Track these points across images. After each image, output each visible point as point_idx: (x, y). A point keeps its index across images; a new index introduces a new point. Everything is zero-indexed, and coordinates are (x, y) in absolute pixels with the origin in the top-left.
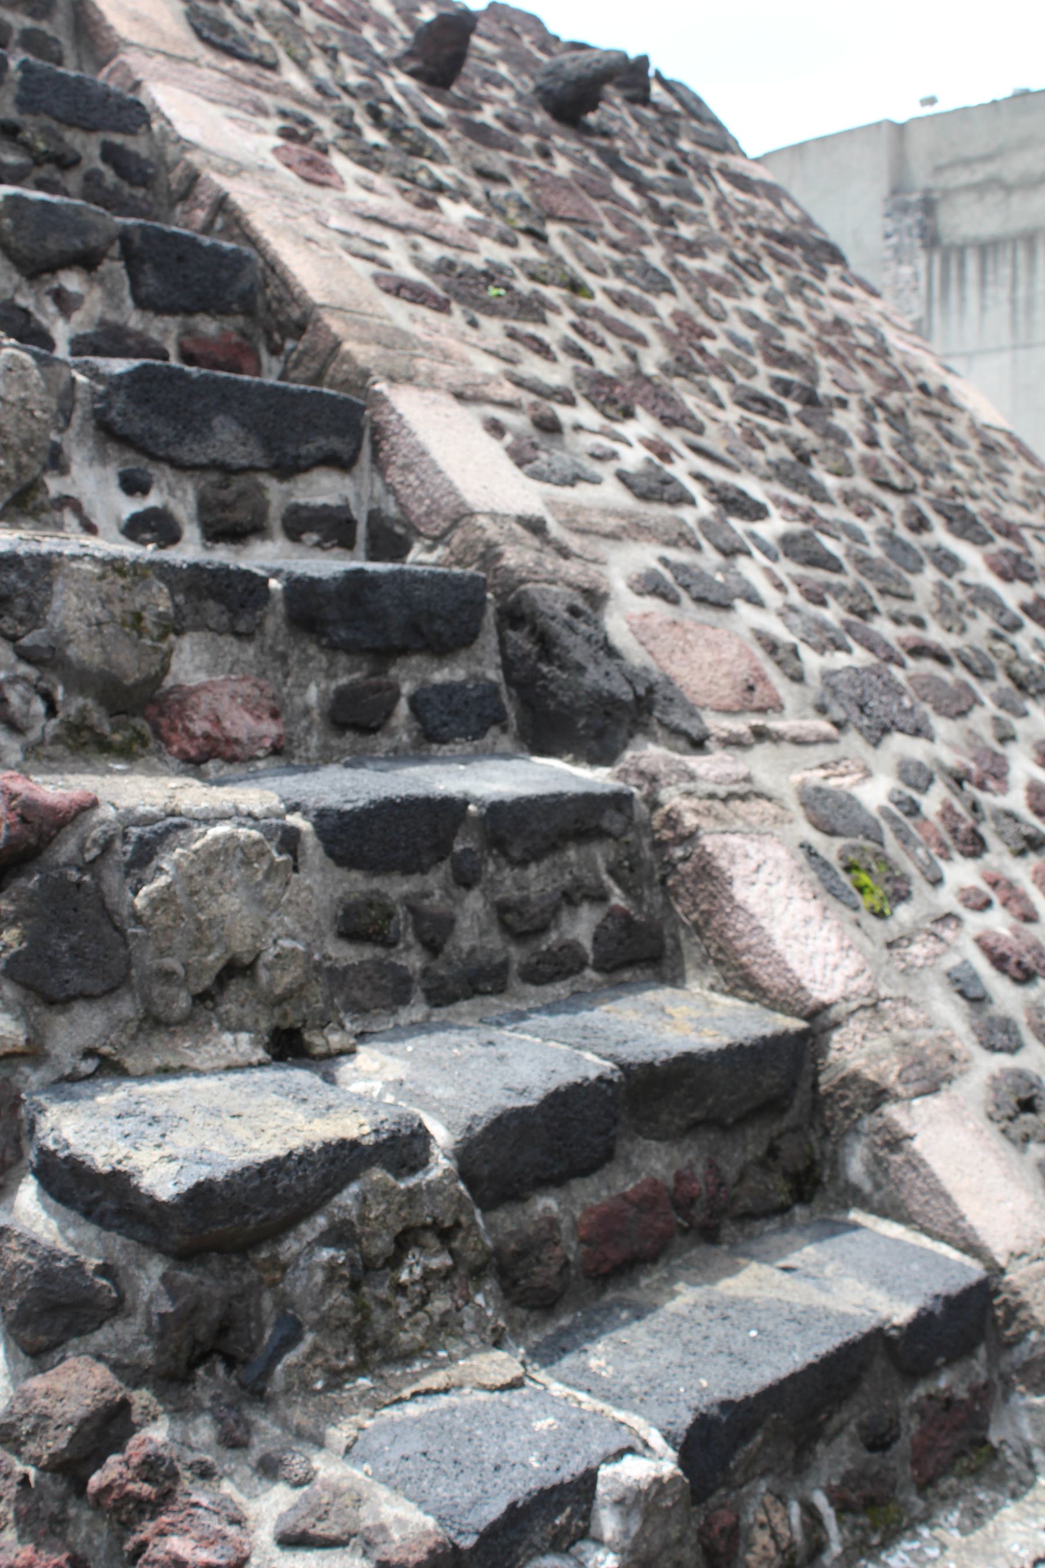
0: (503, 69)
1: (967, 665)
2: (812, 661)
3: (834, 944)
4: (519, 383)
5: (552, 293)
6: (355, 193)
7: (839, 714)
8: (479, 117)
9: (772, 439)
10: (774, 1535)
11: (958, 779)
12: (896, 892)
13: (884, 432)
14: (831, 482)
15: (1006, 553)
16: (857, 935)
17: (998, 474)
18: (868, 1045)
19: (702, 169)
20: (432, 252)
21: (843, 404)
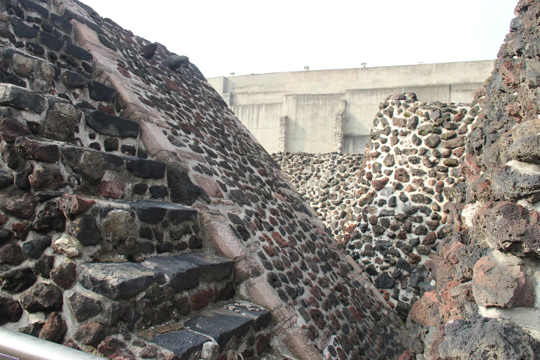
0: (159, 57)
1: (256, 192)
2: (229, 188)
3: (237, 245)
4: (169, 124)
5: (173, 106)
6: (134, 80)
8: (155, 66)
13: (237, 143)
14: (229, 152)
15: (262, 170)
17: (259, 153)
19: (199, 83)
20: (150, 94)
21: (229, 136)
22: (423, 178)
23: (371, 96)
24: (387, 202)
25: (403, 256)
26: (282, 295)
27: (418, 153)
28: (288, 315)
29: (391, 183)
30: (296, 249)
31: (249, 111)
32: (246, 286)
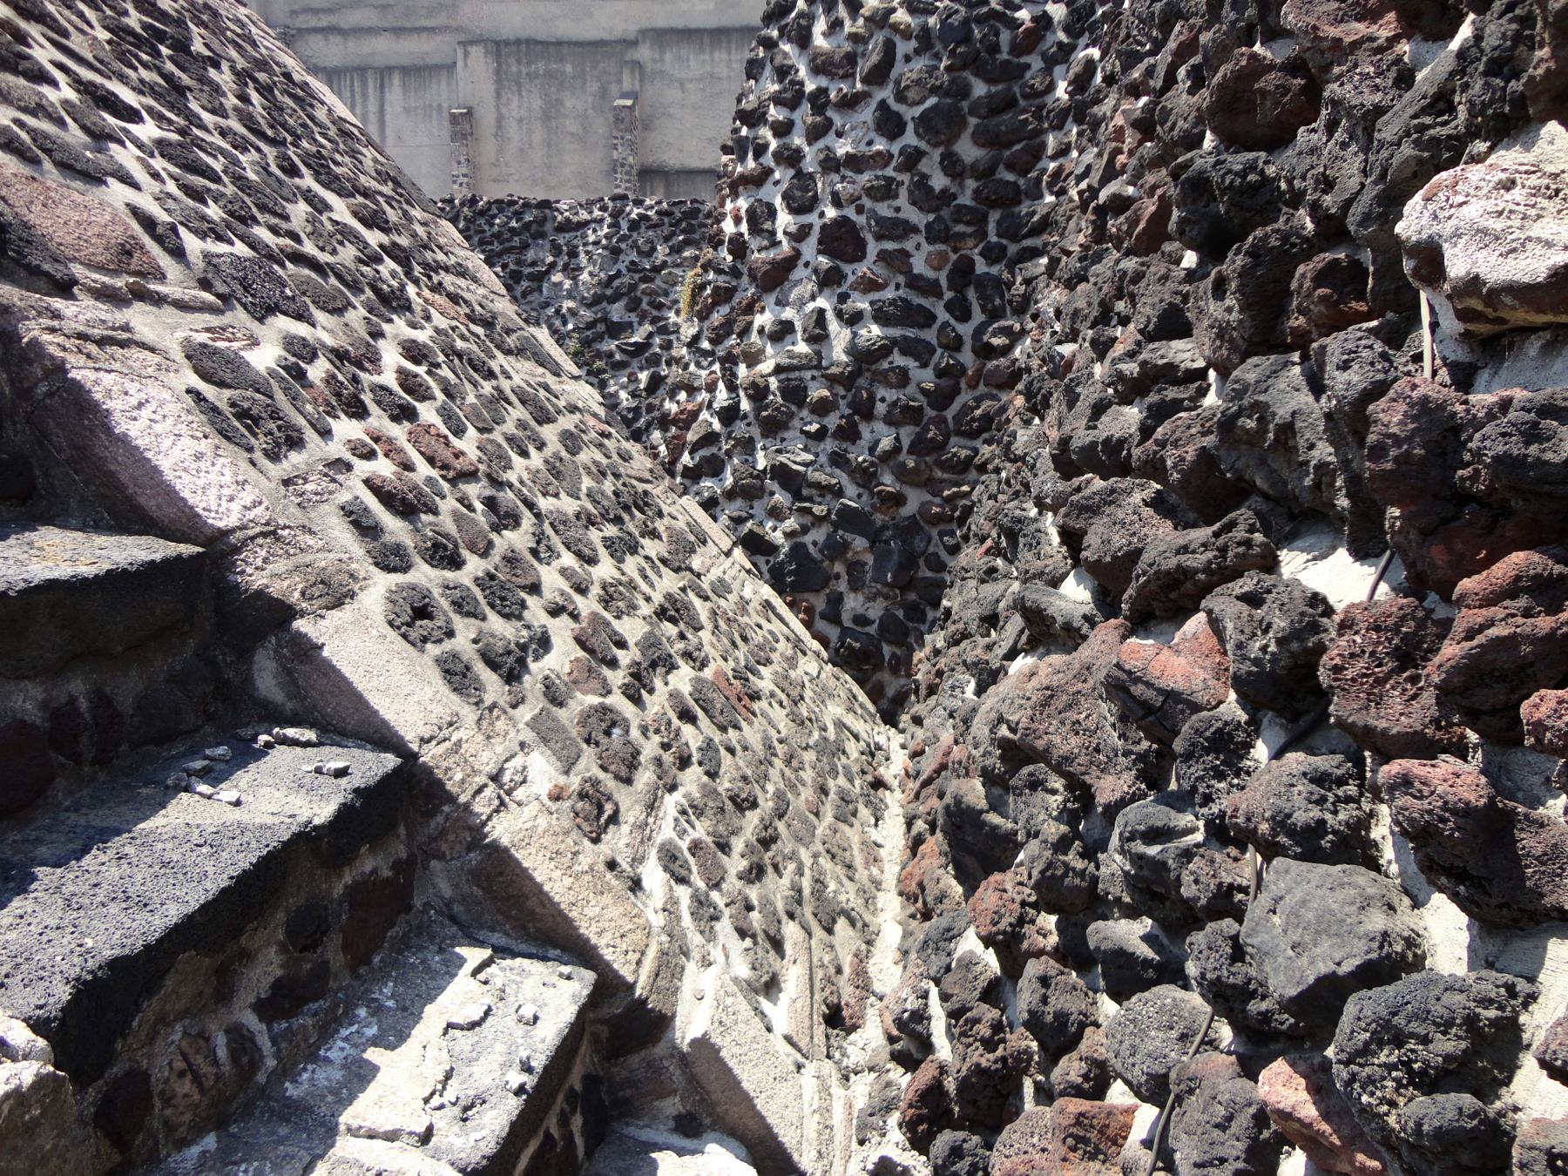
2: (193, 244)
3: (228, 479)
7: (222, 288)
9: (145, 65)
10: (197, 1079)
11: (339, 356)
12: (289, 438)
13: (255, 97)
14: (207, 117)
15: (366, 206)
16: (253, 474)
18: (270, 567)
21: (217, 66)
22: (909, 245)
23: (711, 53)
24: (798, 326)
25: (851, 489)
26: (456, 675)
27: (894, 164)
28: (487, 761)
29: (807, 264)
30: (511, 486)
31: (352, 91)
32: (279, 657)
